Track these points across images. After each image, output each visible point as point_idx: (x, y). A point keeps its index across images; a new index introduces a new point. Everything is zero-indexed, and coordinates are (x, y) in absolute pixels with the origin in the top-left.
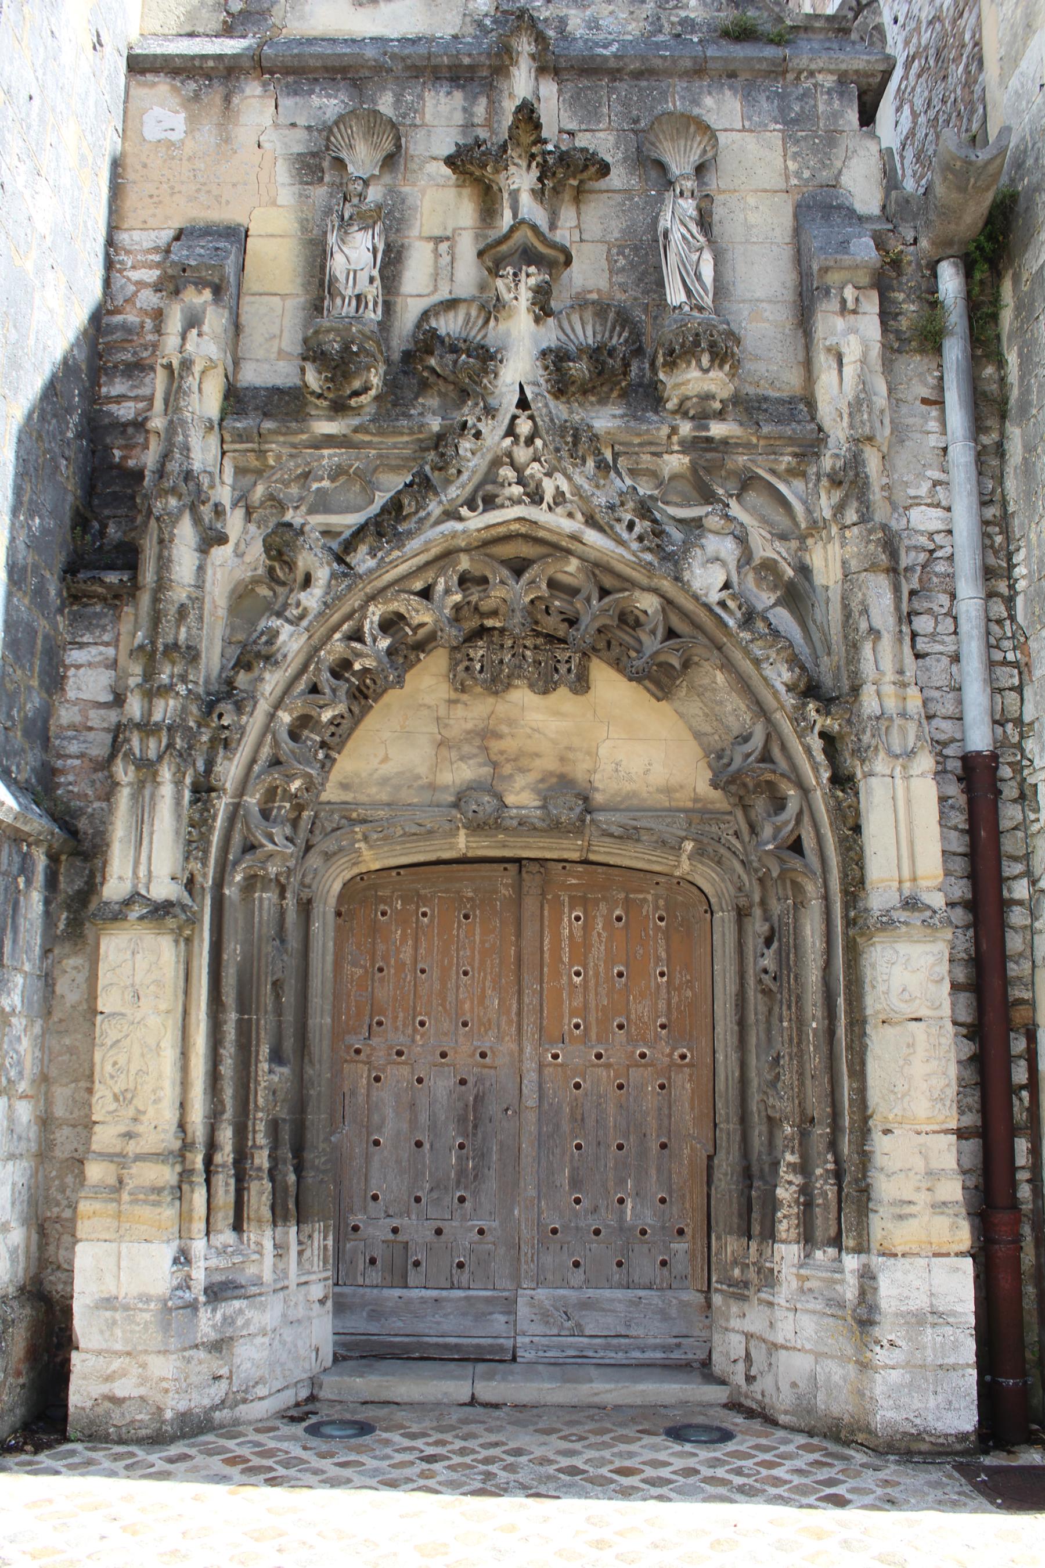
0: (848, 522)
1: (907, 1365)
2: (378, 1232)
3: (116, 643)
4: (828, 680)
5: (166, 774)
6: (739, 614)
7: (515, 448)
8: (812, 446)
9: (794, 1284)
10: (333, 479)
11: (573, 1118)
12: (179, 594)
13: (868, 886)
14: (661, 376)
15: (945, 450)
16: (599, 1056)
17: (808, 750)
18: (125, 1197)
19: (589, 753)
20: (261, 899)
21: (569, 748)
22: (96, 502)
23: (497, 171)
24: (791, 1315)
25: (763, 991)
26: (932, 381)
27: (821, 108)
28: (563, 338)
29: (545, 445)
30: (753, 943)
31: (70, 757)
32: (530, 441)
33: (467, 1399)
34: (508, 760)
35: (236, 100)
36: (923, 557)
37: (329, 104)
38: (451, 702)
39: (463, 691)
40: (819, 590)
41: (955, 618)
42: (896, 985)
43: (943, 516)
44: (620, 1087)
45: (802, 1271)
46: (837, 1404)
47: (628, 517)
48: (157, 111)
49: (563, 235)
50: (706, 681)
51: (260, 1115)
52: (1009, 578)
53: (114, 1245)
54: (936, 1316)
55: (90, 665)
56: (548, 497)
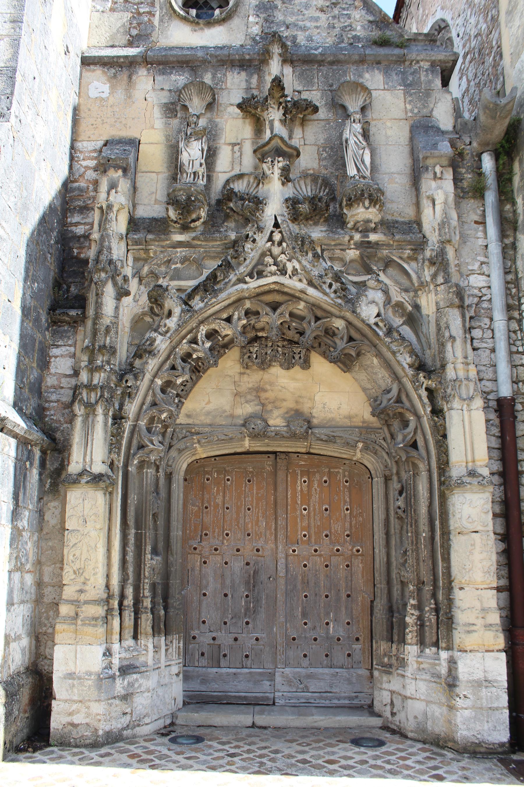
0: (439, 283)
1: (473, 707)
2: (205, 639)
3: (75, 345)
4: (429, 362)
5: (100, 410)
6: (385, 329)
7: (273, 247)
8: (420, 244)
9: (415, 666)
10: (182, 263)
11: (303, 582)
12: (106, 321)
13: (450, 465)
14: (345, 211)
15: (486, 246)
16: (316, 551)
17: (420, 397)
18: (79, 622)
19: (310, 399)
20: (147, 472)
21: (300, 397)
22: (65, 275)
23: (263, 111)
24: (414, 682)
25: (398, 518)
26: (479, 212)
27: (423, 78)
28: (296, 192)
29: (287, 246)
30: (393, 494)
31: (52, 402)
32: (280, 244)
33: (250, 724)
34: (270, 403)
35: (134, 78)
36: (476, 300)
37: (180, 79)
38: (241, 374)
39: (247, 368)
40: (424, 317)
41: (493, 330)
42: (465, 515)
43: (486, 279)
44: (327, 566)
45: (419, 659)
46: (438, 727)
47: (329, 281)
48: (96, 83)
49: (295, 142)
50: (369, 363)
51: (146, 581)
52: (519, 310)
53: (74, 646)
54: (488, 682)
55: (62, 356)
56: (289, 272)
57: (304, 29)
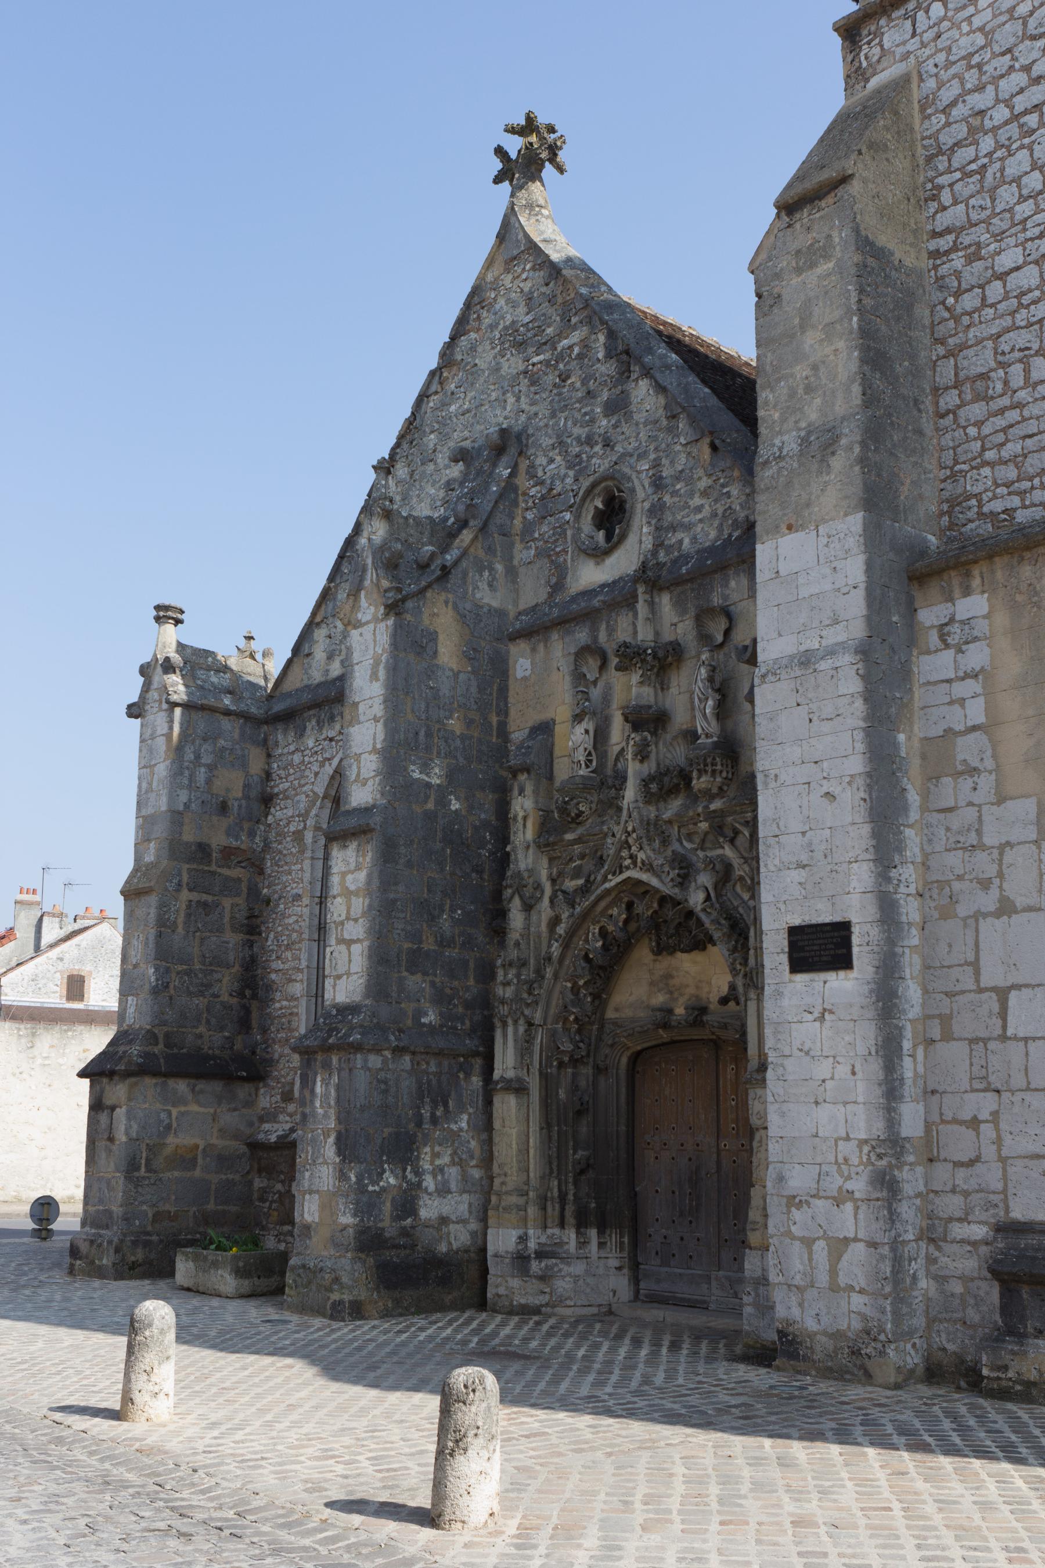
57: (688, 527)
